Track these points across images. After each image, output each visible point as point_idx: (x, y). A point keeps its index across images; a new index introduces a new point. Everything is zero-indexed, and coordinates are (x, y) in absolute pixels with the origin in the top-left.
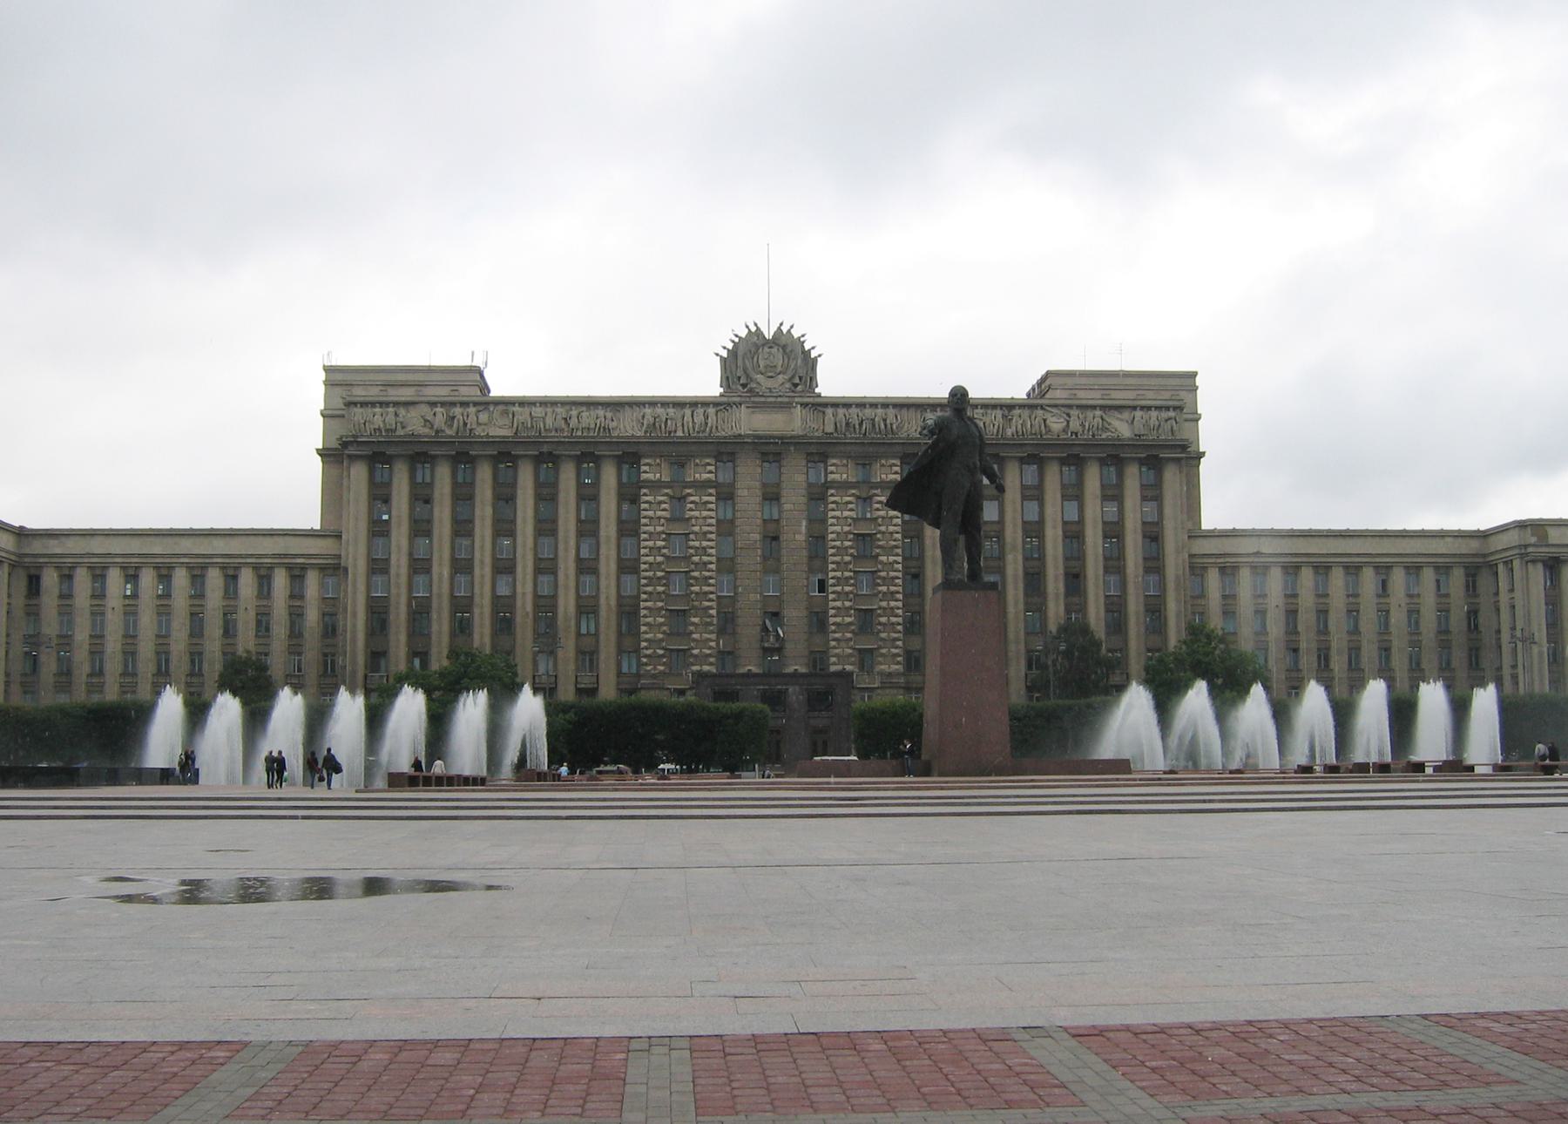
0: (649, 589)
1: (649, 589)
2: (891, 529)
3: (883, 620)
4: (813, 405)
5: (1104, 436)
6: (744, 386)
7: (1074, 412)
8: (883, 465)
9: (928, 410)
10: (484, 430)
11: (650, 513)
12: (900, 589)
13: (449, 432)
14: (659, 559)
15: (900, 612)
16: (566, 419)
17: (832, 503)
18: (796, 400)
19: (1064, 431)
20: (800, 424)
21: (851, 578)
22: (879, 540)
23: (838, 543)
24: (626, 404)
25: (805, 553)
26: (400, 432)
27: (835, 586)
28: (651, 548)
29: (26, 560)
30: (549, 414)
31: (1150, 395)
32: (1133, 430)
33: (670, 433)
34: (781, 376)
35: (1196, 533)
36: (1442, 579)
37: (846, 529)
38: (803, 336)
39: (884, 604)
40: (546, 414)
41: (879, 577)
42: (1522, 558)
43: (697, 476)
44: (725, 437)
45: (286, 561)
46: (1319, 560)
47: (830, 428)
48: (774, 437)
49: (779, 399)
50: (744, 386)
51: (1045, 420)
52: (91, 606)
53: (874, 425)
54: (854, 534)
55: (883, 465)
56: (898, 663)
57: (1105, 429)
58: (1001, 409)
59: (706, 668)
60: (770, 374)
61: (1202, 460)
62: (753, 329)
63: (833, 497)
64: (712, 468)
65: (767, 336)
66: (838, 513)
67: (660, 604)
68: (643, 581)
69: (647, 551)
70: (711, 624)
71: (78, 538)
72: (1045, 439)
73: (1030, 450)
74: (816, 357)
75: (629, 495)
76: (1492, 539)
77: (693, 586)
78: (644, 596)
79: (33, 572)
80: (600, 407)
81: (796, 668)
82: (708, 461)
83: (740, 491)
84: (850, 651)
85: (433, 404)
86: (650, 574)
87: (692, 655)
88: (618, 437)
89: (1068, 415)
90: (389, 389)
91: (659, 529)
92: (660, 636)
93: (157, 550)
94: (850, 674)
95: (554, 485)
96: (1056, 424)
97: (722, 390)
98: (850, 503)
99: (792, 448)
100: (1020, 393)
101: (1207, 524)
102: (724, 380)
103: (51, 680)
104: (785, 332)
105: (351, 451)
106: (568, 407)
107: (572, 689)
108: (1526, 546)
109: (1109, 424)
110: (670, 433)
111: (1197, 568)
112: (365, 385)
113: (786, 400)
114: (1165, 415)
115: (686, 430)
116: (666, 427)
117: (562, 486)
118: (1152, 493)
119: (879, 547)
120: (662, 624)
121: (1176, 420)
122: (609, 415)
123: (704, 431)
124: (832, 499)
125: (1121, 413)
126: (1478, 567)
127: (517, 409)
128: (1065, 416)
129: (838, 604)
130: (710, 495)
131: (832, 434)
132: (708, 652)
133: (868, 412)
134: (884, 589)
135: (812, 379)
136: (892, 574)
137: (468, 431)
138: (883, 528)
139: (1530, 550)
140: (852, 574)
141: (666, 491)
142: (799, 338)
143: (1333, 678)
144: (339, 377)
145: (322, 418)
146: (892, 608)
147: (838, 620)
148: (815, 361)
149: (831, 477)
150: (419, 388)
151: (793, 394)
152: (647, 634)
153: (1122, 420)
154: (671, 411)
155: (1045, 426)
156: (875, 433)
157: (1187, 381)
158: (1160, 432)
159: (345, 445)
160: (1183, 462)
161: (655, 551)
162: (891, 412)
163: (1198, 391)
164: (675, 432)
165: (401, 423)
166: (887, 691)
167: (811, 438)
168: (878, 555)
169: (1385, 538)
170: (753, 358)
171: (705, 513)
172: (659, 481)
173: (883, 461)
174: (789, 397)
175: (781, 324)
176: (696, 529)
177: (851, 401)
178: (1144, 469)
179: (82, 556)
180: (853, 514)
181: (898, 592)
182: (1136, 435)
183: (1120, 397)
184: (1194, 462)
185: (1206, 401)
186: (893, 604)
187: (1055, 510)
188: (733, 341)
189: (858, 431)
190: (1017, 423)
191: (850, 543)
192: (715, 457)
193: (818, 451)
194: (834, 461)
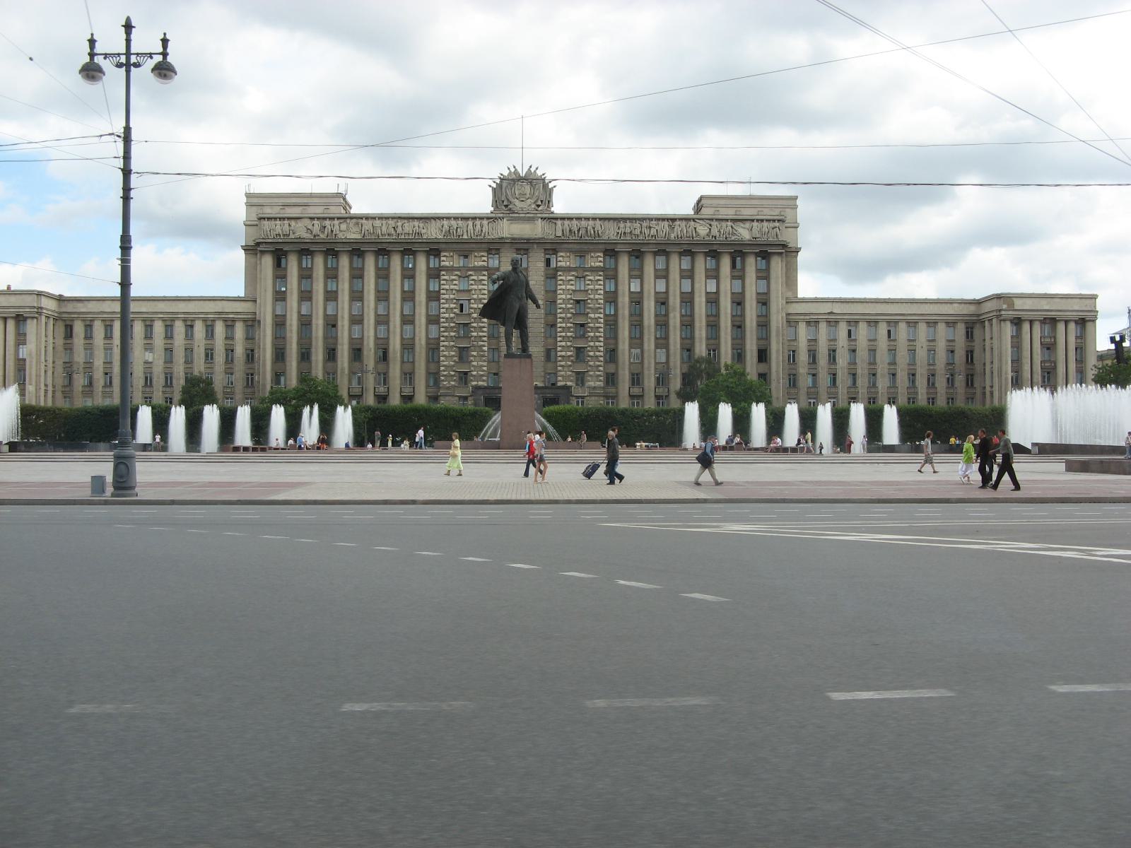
0: (446, 334)
1: (446, 334)
2: (597, 297)
3: (591, 354)
5: (733, 238)
6: (506, 206)
7: (714, 223)
8: (592, 257)
10: (344, 235)
11: (447, 287)
13: (322, 236)
14: (452, 315)
16: (394, 228)
17: (561, 280)
20: (540, 230)
21: (571, 327)
23: (563, 306)
26: (292, 236)
29: (64, 316)
30: (384, 225)
31: (766, 211)
34: (529, 200)
35: (793, 300)
36: (853, 329)
37: (569, 297)
38: (543, 175)
39: (592, 344)
41: (589, 327)
42: (997, 318)
43: (476, 263)
44: (493, 239)
45: (223, 316)
46: (870, 318)
47: (559, 234)
48: (522, 239)
49: (528, 215)
50: (506, 206)
51: (695, 228)
53: (587, 231)
55: (592, 257)
56: (600, 381)
57: (733, 234)
59: (481, 383)
62: (513, 170)
63: (561, 277)
64: (485, 259)
66: (563, 287)
67: (452, 343)
68: (442, 329)
69: (444, 310)
70: (483, 356)
73: (685, 247)
74: (552, 188)
75: (434, 274)
76: (983, 305)
77: (473, 332)
78: (442, 339)
79: (68, 323)
84: (570, 373)
85: (312, 219)
86: (446, 325)
87: (472, 376)
89: (710, 225)
90: (286, 208)
91: (452, 296)
92: (453, 363)
93: (144, 310)
94: (571, 387)
95: (388, 269)
96: (703, 230)
97: (492, 209)
99: (535, 246)
100: (688, 210)
101: (801, 295)
102: (494, 202)
103: (80, 389)
104: (533, 171)
105: (262, 248)
106: (395, 220)
107: (398, 396)
108: (1000, 310)
110: (459, 236)
111: (791, 322)
112: (271, 206)
113: (532, 215)
114: (772, 225)
117: (392, 269)
118: (764, 275)
119: (590, 308)
120: (453, 356)
122: (421, 225)
123: (480, 235)
126: (974, 323)
127: (364, 221)
128: (708, 226)
129: (563, 344)
130: (484, 275)
132: (482, 373)
133: (584, 223)
134: (592, 334)
135: (549, 203)
136: (597, 325)
138: (592, 296)
139: (1003, 313)
141: (456, 273)
142: (541, 176)
143: (878, 392)
144: (255, 201)
147: (563, 353)
148: (551, 191)
149: (559, 264)
150: (305, 207)
152: (444, 362)
153: (744, 228)
154: (460, 222)
155: (696, 232)
156: (588, 236)
158: (770, 234)
159: (258, 244)
160: (784, 255)
161: (449, 310)
162: (598, 222)
164: (462, 235)
165: (293, 230)
166: (593, 398)
167: (547, 239)
168: (588, 313)
169: (915, 304)
171: (480, 287)
172: (452, 266)
173: (592, 254)
175: (531, 167)
176: (475, 296)
178: (759, 259)
179: (99, 313)
180: (573, 288)
183: (747, 213)
184: (794, 254)
186: (597, 344)
187: (703, 287)
192: (487, 251)
193: (551, 248)
194: (562, 254)
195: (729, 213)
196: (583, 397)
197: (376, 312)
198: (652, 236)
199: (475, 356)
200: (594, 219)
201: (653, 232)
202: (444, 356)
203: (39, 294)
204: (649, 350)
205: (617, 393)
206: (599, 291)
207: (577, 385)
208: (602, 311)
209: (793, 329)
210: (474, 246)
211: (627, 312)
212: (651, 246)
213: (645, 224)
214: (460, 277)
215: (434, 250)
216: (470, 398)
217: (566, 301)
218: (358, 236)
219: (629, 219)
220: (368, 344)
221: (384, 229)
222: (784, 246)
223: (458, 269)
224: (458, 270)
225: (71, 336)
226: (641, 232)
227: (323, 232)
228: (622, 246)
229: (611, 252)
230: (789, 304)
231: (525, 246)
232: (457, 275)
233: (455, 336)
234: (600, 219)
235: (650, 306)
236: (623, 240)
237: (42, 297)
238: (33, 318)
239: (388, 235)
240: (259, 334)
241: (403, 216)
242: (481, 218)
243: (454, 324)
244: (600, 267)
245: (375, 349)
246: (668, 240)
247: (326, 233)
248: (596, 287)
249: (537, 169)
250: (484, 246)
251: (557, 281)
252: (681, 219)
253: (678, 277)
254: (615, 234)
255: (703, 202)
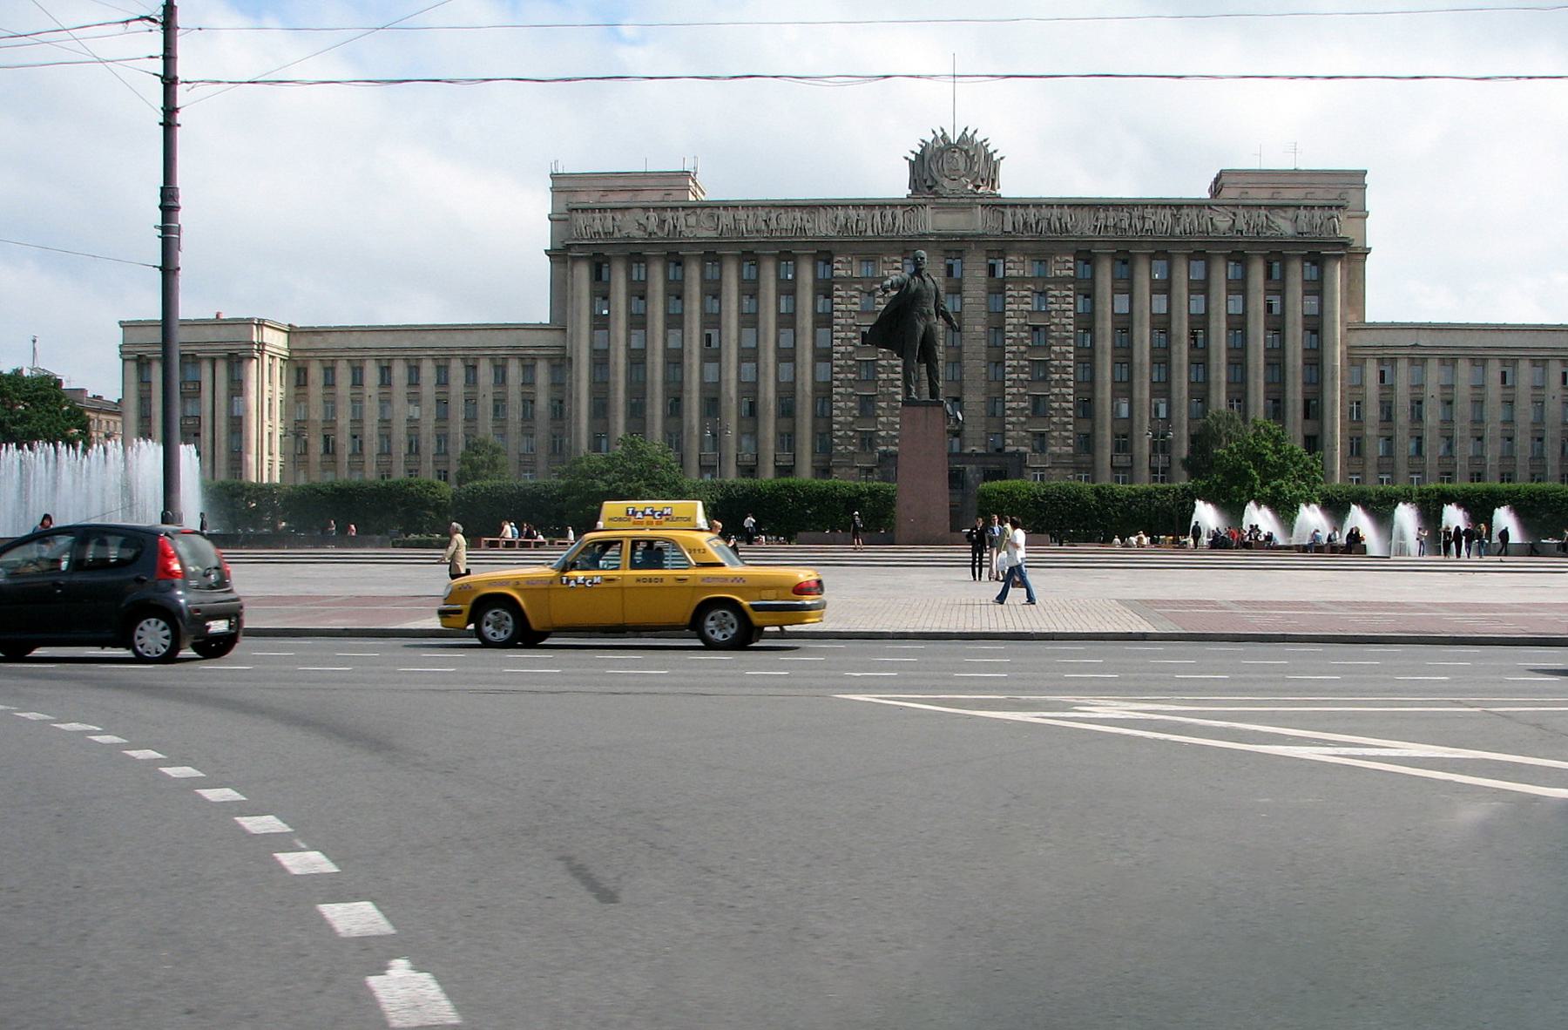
0: (841, 376)
1: (841, 376)
2: (1064, 321)
3: (1056, 405)
4: (993, 205)
5: (1268, 234)
6: (930, 188)
7: (1240, 212)
8: (1057, 262)
9: (1101, 210)
10: (692, 232)
11: (843, 307)
12: (1072, 377)
13: (660, 234)
14: (850, 349)
15: (1071, 398)
18: (977, 201)
19: (1229, 229)
20: (980, 224)
21: (1026, 366)
22: (1053, 331)
24: (820, 206)
25: (984, 343)
26: (617, 235)
27: (1011, 373)
28: (842, 339)
32: (1296, 228)
33: (861, 232)
37: (1022, 321)
39: (1056, 391)
40: (748, 217)
41: (1052, 366)
47: (1009, 228)
48: (953, 236)
49: (962, 201)
50: (930, 188)
51: (1211, 219)
52: (352, 394)
53: (1049, 224)
54: (1029, 325)
55: (1057, 262)
56: (1069, 445)
58: (1170, 208)
59: (892, 448)
60: (953, 177)
61: (1368, 256)
62: (940, 134)
64: (899, 265)
65: (952, 142)
67: (850, 390)
68: (836, 369)
69: (839, 341)
72: (1211, 237)
73: (1198, 247)
75: (824, 289)
78: (836, 383)
80: (797, 210)
81: (974, 448)
82: (895, 258)
83: (966, 286)
85: (646, 209)
87: (879, 437)
88: (814, 237)
89: (1234, 214)
92: (851, 419)
94: (1026, 453)
96: (1223, 222)
97: (910, 192)
98: (1026, 296)
101: (1370, 317)
106: (767, 210)
109: (1273, 223)
110: (861, 232)
111: (1355, 358)
113: (969, 201)
114: (1327, 213)
115: (876, 230)
116: (857, 226)
118: (1316, 288)
120: (852, 408)
121: (1338, 219)
122: (805, 217)
123: (892, 231)
124: (1009, 293)
125: (1285, 212)
127: (721, 211)
129: (1014, 390)
131: (1010, 232)
132: (894, 433)
133: (1045, 212)
134: (1057, 376)
137: (678, 234)
138: (1057, 321)
140: (1027, 363)
141: (857, 286)
142: (982, 143)
143: (1485, 465)
144: (564, 184)
145: (550, 222)
146: (1064, 395)
147: (1014, 405)
148: (996, 165)
149: (1008, 273)
151: (974, 196)
154: (862, 212)
155: (1212, 224)
156: (1051, 232)
157: (1356, 180)
159: (568, 247)
160: (1345, 259)
163: (1367, 190)
164: (866, 230)
165: (618, 227)
167: (990, 236)
168: (1052, 345)
170: (938, 162)
173: (1058, 258)
174: (971, 198)
175: (966, 129)
177: (1028, 202)
178: (1308, 264)
179: (343, 350)
180: (1029, 307)
181: (1070, 380)
182: (1299, 233)
183: (1289, 196)
184: (1362, 257)
185: (1373, 200)
186: (1064, 390)
187: (1223, 305)
188: (921, 146)
189: (1034, 230)
190: (1185, 221)
191: (1026, 334)
192: (902, 255)
193: (998, 247)
195: (1263, 196)
196: (1042, 469)
197: (739, 343)
198: (1147, 230)
199: (884, 408)
200: (1061, 206)
201: (1149, 225)
202: (838, 408)
204: (1141, 400)
205: (1093, 462)
206: (1068, 313)
207: (1034, 451)
208: (1072, 342)
209: (1356, 370)
210: (883, 245)
211: (1108, 344)
212: (1144, 245)
213: (1136, 213)
214: (861, 292)
215: (824, 253)
216: (876, 470)
217: (1019, 328)
218: (713, 234)
219: (1112, 205)
220: (728, 393)
221: (750, 223)
222: (1345, 244)
223: (860, 280)
224: (861, 283)
226: (1130, 225)
227: (663, 229)
228: (1102, 245)
229: (1086, 256)
230: (1351, 333)
231: (958, 246)
232: (856, 290)
233: (854, 379)
234: (1070, 206)
235: (1143, 336)
236: (1103, 237)
239: (757, 231)
240: (571, 377)
241: (777, 203)
242: (893, 206)
243: (853, 362)
244: (1069, 276)
245: (738, 398)
246: (1172, 235)
247: (666, 229)
248: (1064, 306)
249: (975, 132)
250: (896, 245)
251: (1004, 298)
252: (1189, 206)
253: (1185, 291)
254: (1092, 228)
255: (1223, 179)
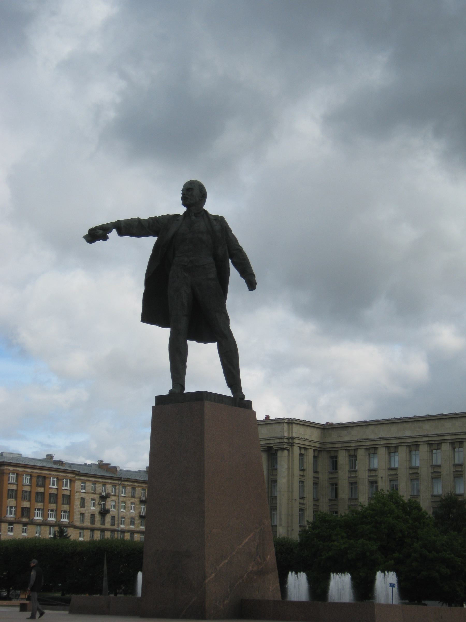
52: (369, 476)
71: (359, 428)
79: (333, 454)
93: (408, 434)
203: (291, 422)
225: (336, 469)
237: (294, 425)
238: (283, 449)
